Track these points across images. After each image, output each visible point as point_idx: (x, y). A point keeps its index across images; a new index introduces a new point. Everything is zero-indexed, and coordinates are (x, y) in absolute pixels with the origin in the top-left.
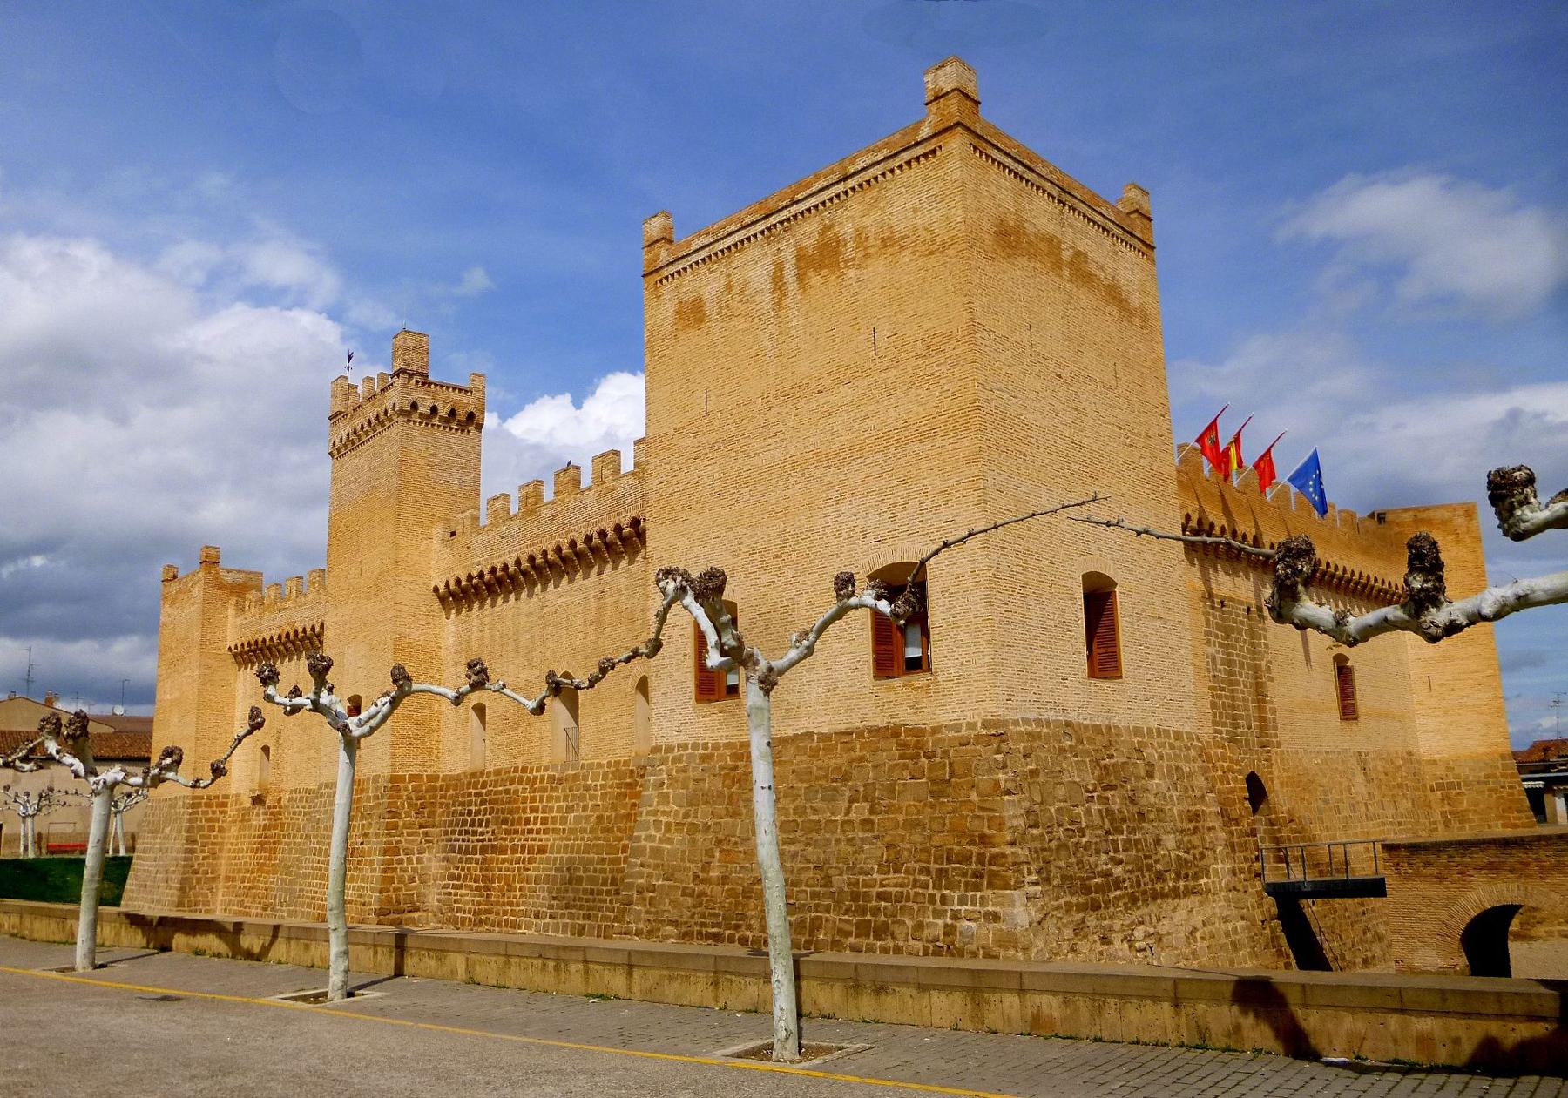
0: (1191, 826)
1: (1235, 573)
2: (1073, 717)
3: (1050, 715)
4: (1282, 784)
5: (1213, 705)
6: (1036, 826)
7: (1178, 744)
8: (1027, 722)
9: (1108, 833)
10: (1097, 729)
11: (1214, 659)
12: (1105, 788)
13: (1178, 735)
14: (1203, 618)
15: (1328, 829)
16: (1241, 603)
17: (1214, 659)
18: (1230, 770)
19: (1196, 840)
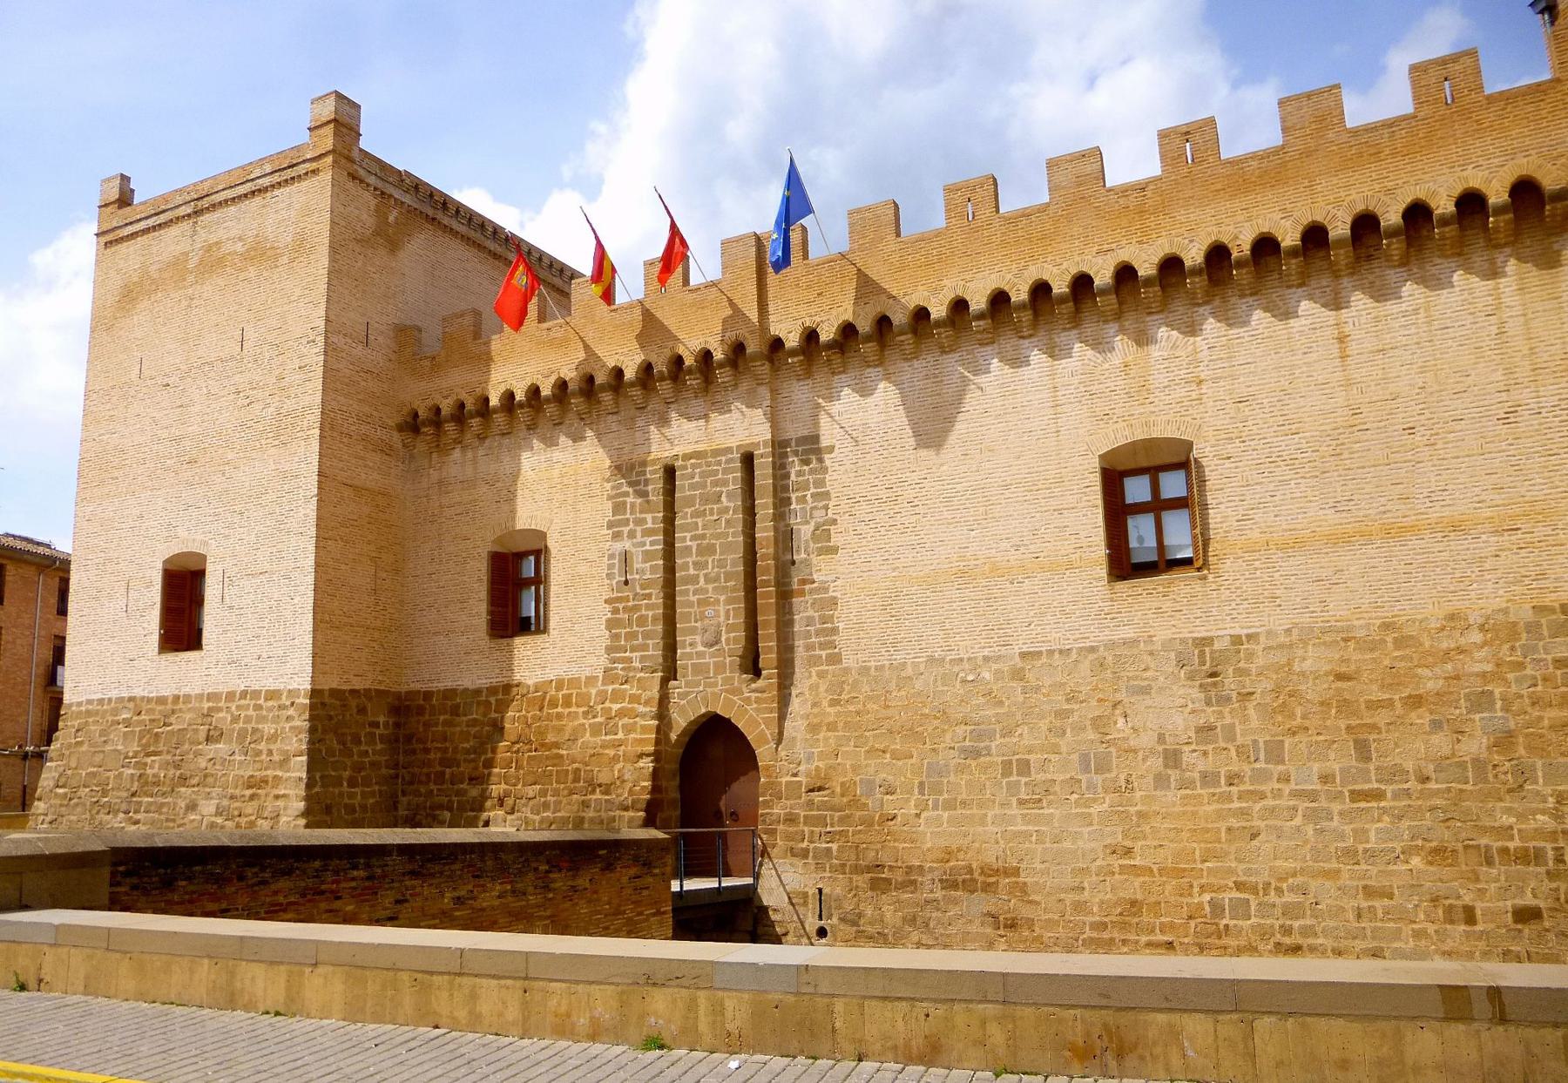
0: (248, 792)
1: (724, 409)
2: (138, 692)
3: (114, 694)
4: (813, 728)
5: (611, 624)
6: (63, 786)
7: (270, 703)
8: (89, 702)
9: (133, 795)
10: (161, 700)
11: (626, 558)
12: (148, 755)
13: (273, 695)
14: (609, 505)
15: (950, 805)
16: (729, 450)
17: (626, 558)
18: (621, 713)
19: (250, 808)
